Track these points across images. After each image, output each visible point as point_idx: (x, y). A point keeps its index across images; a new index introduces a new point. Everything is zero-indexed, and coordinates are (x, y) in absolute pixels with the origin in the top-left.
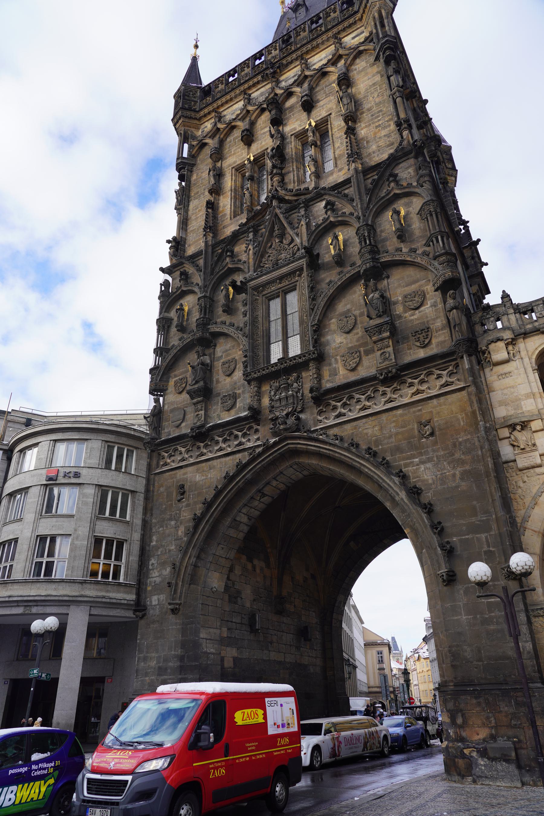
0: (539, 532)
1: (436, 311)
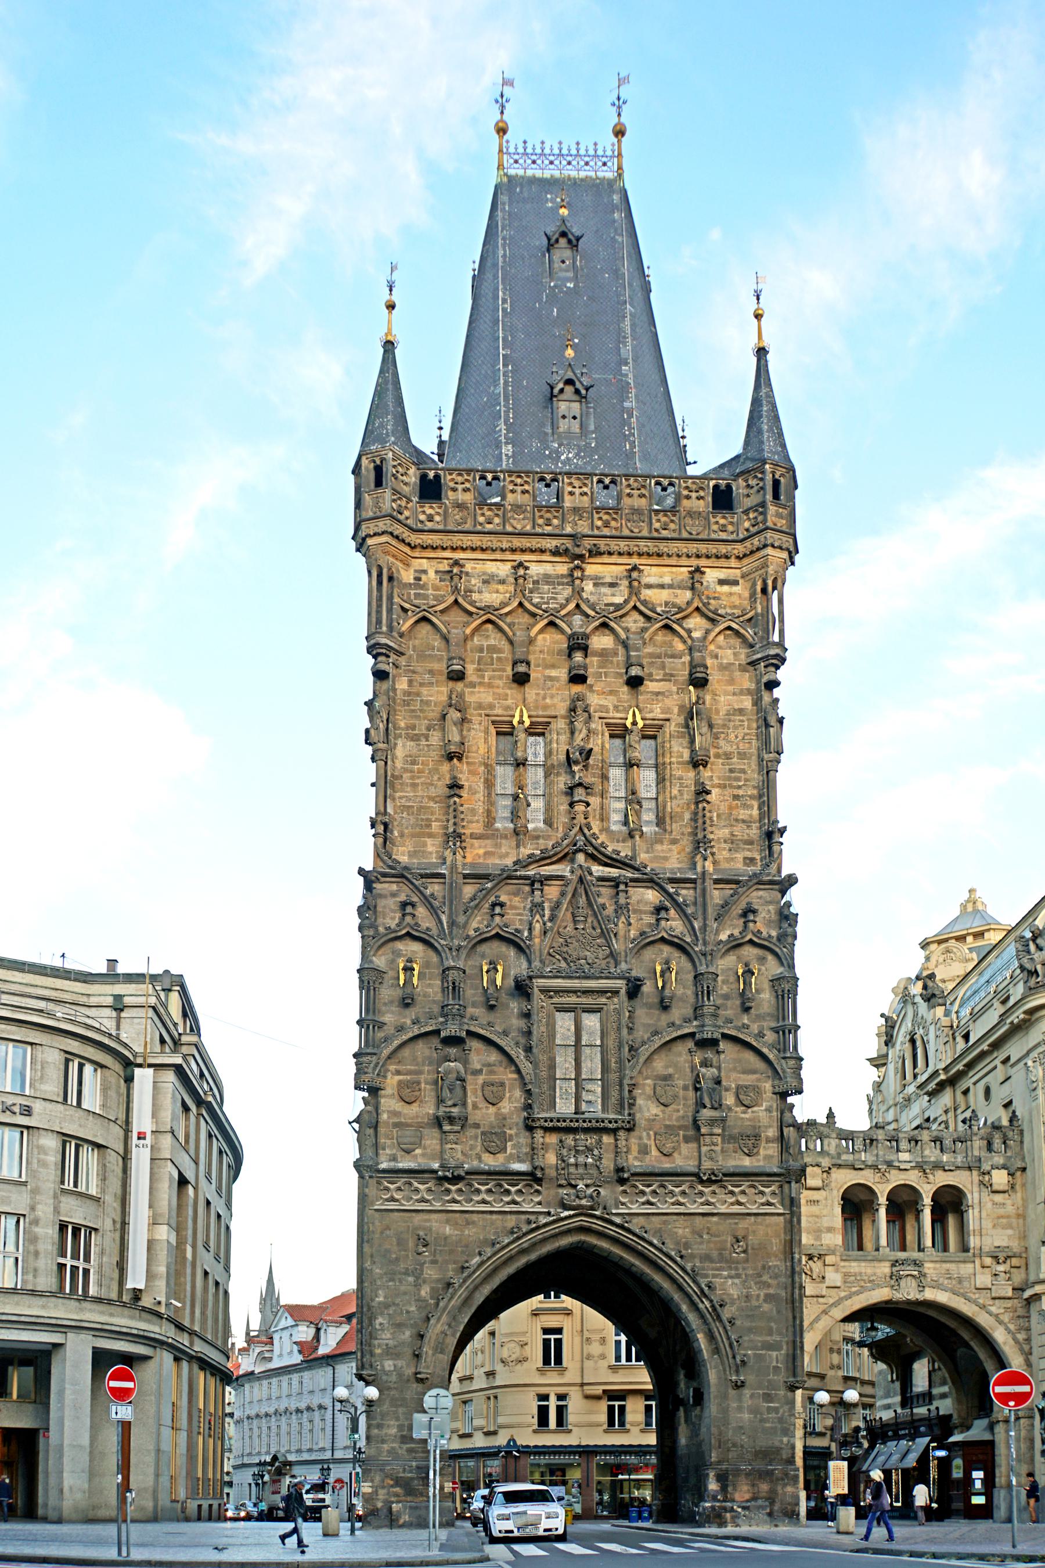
1: (770, 1117)
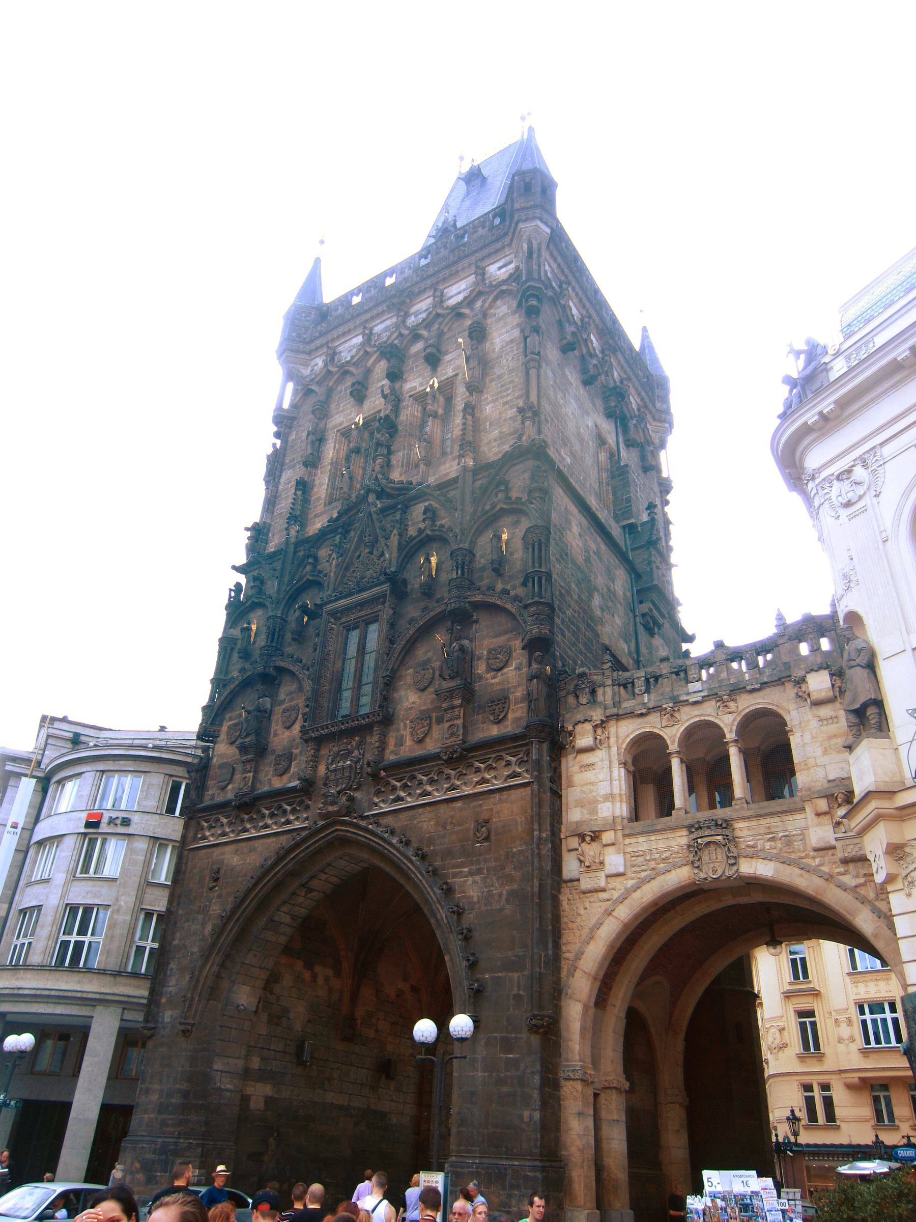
0: (589, 975)
1: (520, 675)
